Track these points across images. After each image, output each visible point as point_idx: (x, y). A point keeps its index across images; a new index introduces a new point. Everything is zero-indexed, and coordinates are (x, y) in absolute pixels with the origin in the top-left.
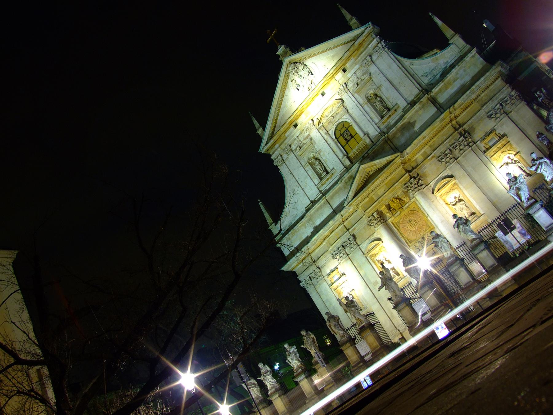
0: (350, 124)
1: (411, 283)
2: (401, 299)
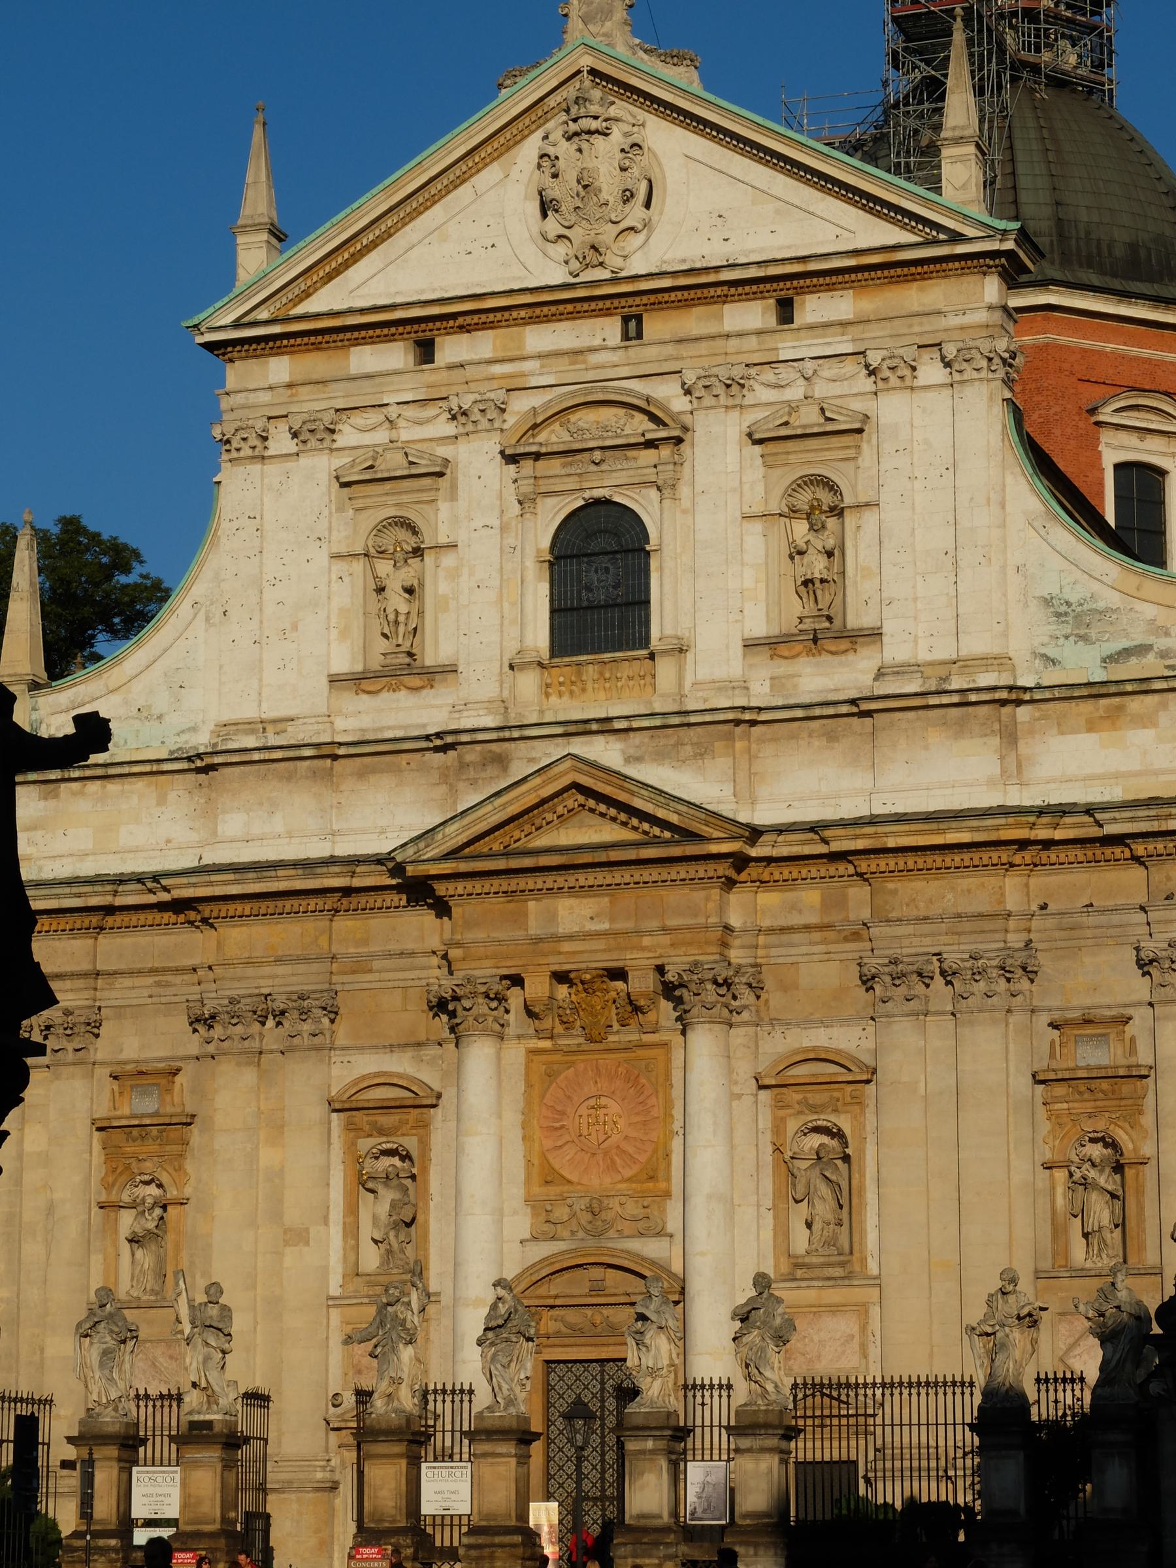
0: (648, 548)
1: (471, 1392)
2: (403, 1422)
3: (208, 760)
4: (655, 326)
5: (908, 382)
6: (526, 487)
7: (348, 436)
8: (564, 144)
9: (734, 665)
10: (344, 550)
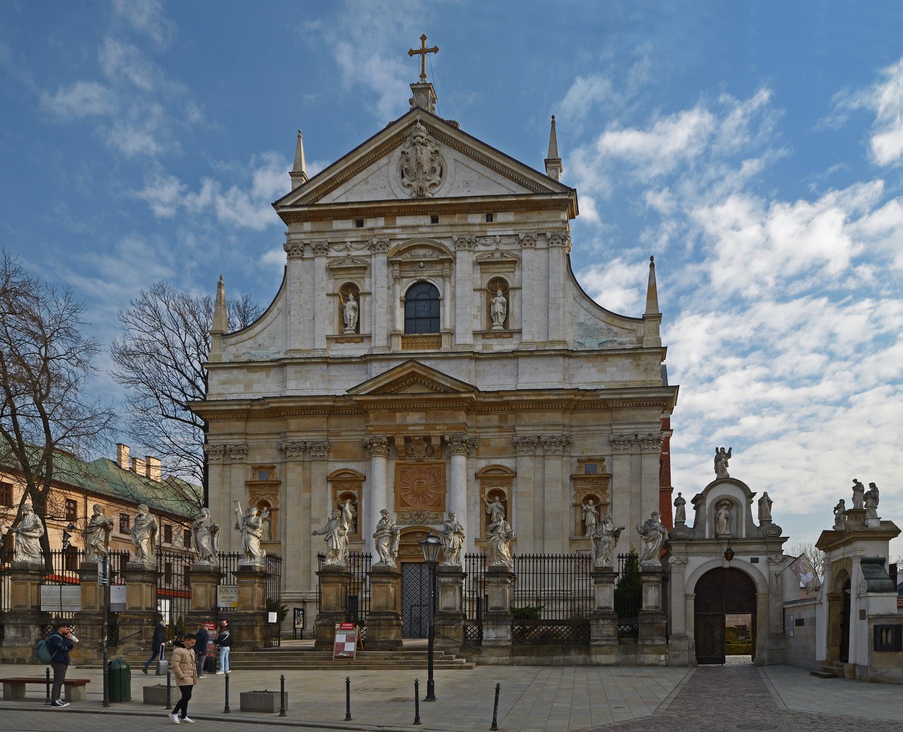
3: (283, 361)
4: (442, 220)
5: (533, 246)
6: (397, 273)
7: (333, 253)
8: (411, 148)
9: (469, 340)
10: (331, 292)
